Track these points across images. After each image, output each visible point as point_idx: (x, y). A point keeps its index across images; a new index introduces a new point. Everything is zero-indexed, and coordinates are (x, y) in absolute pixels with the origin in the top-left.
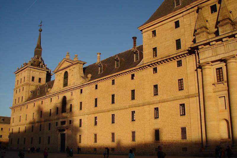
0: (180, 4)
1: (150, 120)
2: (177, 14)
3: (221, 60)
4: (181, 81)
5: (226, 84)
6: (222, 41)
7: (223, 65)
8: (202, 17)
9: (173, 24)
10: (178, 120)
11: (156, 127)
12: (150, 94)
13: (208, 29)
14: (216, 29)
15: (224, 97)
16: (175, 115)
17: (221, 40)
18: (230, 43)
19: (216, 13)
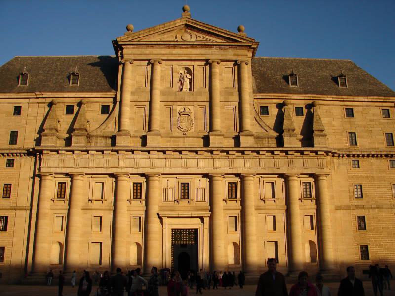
0: (27, 85)
3: (67, 174)
4: (8, 186)
5: (67, 202)
6: (73, 154)
7: (67, 180)
8: (54, 115)
13: (58, 132)
14: (68, 135)
15: (63, 216)
18: (81, 157)
19: (72, 117)
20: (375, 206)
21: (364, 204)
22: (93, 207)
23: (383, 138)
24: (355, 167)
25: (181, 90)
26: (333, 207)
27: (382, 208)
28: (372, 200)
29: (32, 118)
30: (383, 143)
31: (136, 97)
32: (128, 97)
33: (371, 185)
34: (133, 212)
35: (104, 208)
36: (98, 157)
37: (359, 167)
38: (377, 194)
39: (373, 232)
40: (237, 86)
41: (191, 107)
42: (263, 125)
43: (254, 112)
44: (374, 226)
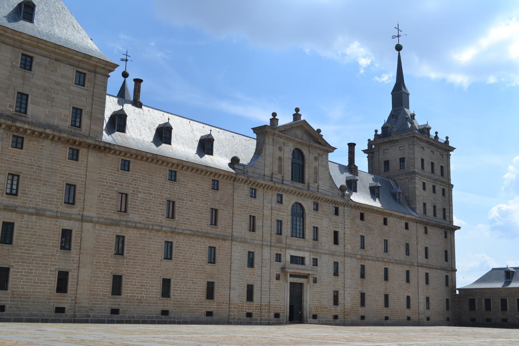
20: (33, 211)
21: (17, 204)
23: (68, 113)
24: (16, 147)
27: (44, 215)
28: (30, 201)
30: (67, 121)
33: (34, 179)
37: (22, 148)
38: (40, 193)
39: (22, 249)
44: (25, 240)
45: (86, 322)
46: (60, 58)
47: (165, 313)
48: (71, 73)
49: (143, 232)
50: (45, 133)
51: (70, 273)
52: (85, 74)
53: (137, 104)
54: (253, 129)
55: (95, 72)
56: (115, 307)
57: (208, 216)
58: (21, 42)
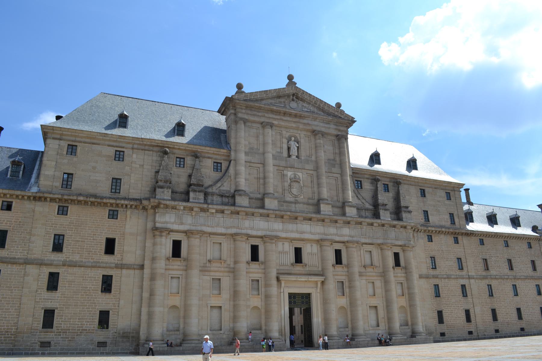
1: (37, 291)
2: (124, 140)
9: (111, 151)
10: (96, 298)
11: (49, 305)
12: (45, 246)
16: (93, 290)
17: (191, 209)
20: (445, 276)
21: (438, 274)
22: (212, 269)
23: (447, 217)
25: (289, 156)
26: (418, 276)
29: (138, 166)
31: (249, 158)
32: (242, 157)
34: (251, 275)
35: (223, 269)
36: (217, 216)
37: (432, 241)
40: (338, 159)
41: (300, 174)
42: (361, 198)
43: (353, 185)
45: (484, 339)
46: (436, 186)
47: (522, 329)
48: (443, 194)
49: (500, 281)
50: (441, 231)
51: (470, 310)
52: (449, 193)
53: (471, 204)
54: (538, 206)
55: (454, 191)
56: (497, 328)
57: (530, 265)
58: (418, 182)
